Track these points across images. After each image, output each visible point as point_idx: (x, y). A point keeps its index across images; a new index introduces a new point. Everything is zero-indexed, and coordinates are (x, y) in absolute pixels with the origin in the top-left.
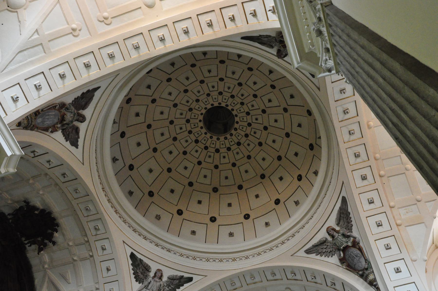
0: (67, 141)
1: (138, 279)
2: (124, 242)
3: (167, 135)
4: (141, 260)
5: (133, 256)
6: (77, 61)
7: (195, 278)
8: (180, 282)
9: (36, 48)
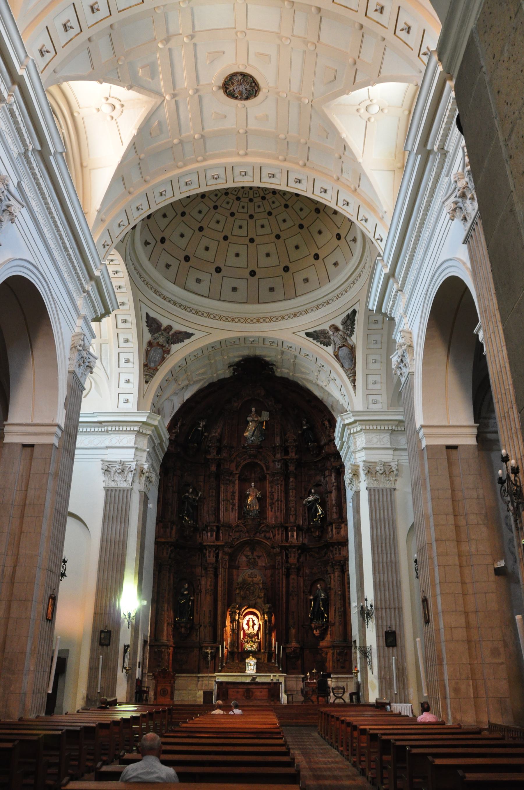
0: (183, 341)
1: (327, 344)
2: (293, 333)
3: (244, 223)
4: (315, 332)
5: (308, 334)
6: (119, 327)
7: (356, 307)
8: (351, 320)
9: (102, 349)
